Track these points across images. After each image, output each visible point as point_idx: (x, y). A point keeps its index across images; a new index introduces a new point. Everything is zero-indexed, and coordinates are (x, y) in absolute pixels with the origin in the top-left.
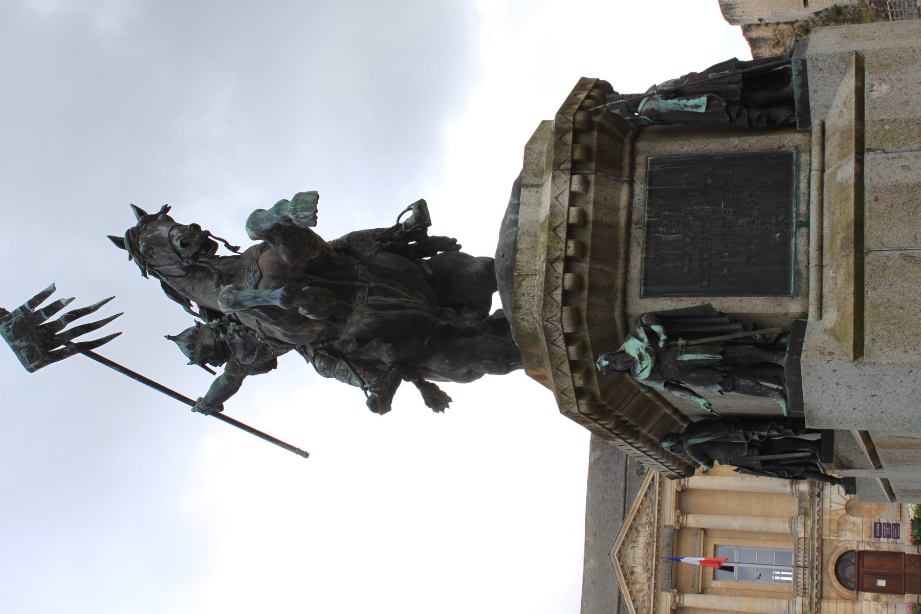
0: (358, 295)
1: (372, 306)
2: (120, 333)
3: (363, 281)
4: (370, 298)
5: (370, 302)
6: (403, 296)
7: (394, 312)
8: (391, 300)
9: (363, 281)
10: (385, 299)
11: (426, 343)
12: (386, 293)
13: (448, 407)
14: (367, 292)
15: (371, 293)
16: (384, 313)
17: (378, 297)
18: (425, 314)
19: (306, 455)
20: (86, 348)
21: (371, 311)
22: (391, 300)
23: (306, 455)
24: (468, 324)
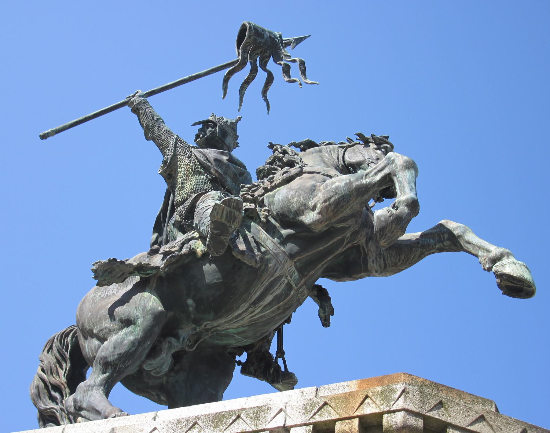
0: (296, 273)
1: (280, 277)
2: (224, 98)
3: (301, 287)
4: (286, 281)
5: (283, 279)
6: (261, 312)
7: (258, 294)
8: (269, 298)
9: (301, 287)
10: (274, 294)
11: (190, 302)
12: (277, 299)
13: (96, 278)
14: (292, 283)
15: (289, 287)
16: (266, 283)
17: (281, 290)
18: (223, 321)
19: (44, 137)
20: (238, 66)
21: (277, 274)
22: (269, 298)
23: (44, 137)
24: (163, 355)
